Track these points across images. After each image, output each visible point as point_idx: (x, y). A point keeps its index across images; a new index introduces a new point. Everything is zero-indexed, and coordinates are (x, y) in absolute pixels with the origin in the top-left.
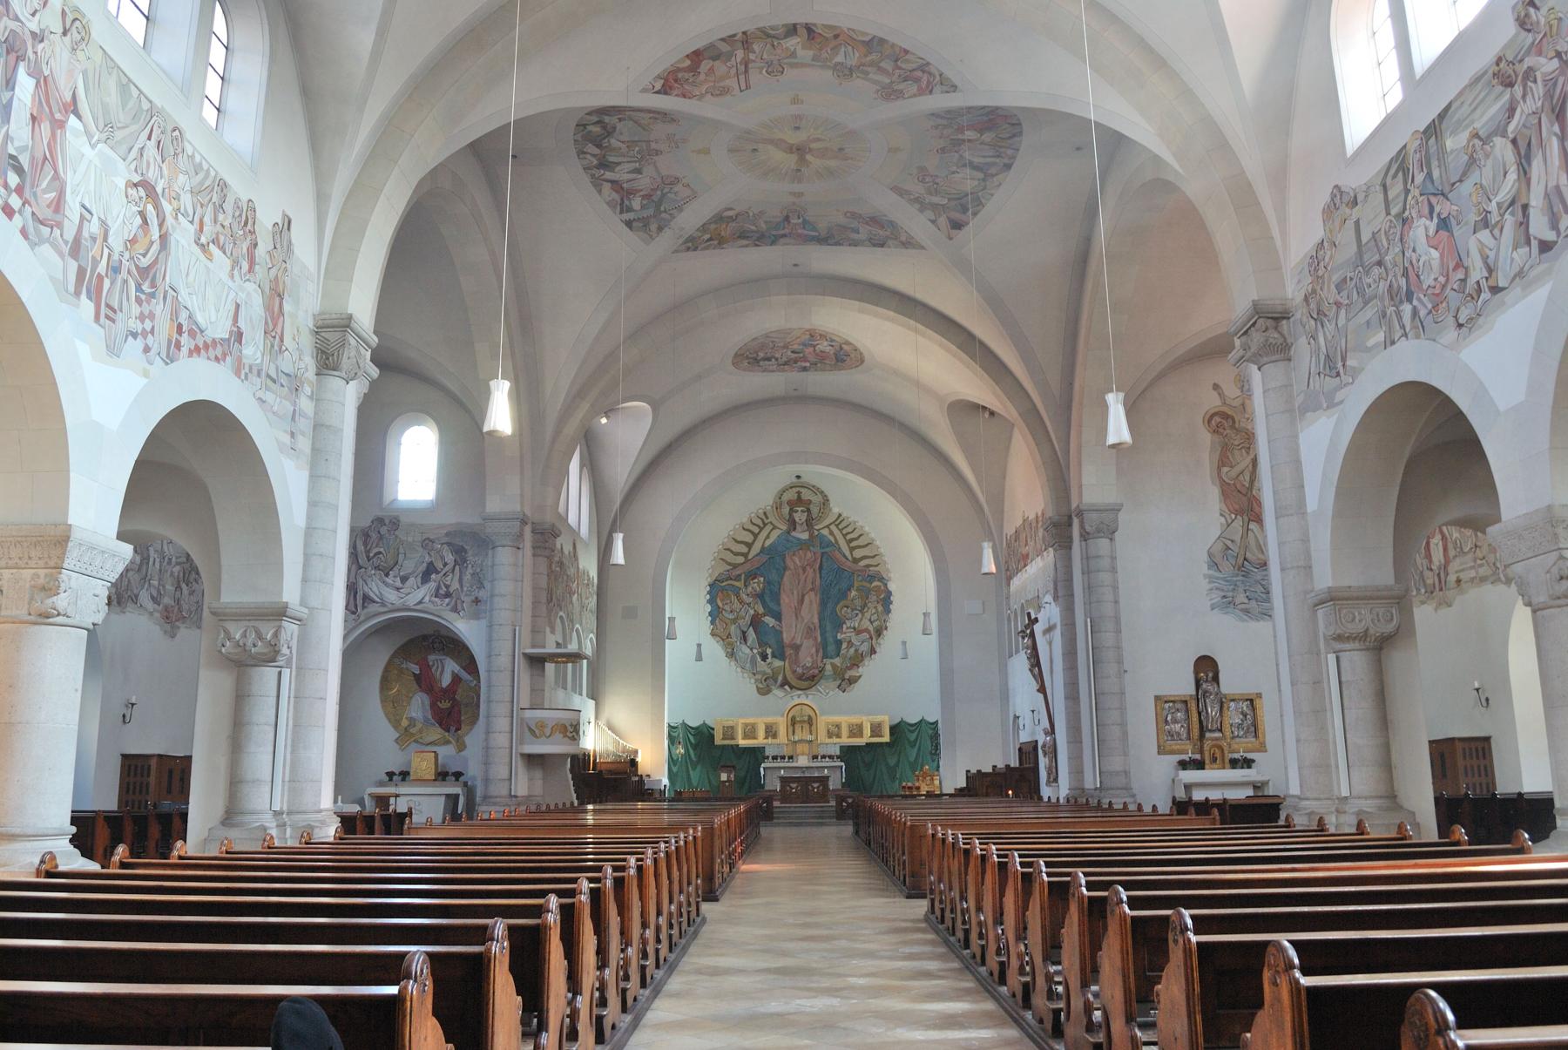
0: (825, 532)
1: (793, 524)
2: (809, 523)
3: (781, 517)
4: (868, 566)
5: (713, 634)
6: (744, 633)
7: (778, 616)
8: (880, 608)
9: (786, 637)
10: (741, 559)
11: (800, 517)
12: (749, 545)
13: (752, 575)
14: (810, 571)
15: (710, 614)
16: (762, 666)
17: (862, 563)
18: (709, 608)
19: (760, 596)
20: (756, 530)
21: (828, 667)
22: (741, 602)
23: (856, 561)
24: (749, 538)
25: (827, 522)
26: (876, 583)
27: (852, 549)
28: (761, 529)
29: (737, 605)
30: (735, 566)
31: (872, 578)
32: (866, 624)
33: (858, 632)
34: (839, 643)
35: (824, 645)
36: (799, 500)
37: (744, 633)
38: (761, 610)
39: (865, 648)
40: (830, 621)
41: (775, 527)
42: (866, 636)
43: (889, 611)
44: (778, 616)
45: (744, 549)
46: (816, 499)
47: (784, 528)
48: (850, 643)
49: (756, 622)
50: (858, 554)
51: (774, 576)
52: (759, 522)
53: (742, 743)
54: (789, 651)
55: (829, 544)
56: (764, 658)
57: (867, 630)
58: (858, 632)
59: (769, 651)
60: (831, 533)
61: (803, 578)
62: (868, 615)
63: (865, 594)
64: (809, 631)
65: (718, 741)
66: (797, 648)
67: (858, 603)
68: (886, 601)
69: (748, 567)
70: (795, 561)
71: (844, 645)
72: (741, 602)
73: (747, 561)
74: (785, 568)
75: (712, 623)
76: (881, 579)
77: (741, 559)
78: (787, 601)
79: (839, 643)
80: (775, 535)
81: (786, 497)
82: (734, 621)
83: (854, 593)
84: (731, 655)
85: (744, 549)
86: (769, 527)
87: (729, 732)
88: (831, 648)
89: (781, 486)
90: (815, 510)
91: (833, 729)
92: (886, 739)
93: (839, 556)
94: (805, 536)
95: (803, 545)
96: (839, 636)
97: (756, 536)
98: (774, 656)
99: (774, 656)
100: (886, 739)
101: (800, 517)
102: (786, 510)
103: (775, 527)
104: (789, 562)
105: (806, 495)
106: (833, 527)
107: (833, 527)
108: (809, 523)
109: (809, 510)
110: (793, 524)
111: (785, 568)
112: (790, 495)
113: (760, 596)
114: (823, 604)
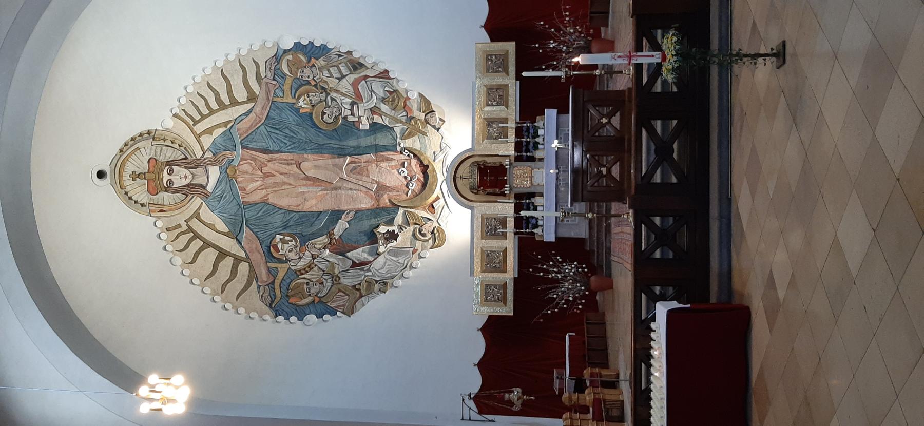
0: (207, 141)
1: (192, 189)
2: (191, 164)
3: (178, 206)
4: (259, 78)
5: (350, 312)
6: (354, 265)
7: (337, 215)
8: (321, 62)
9: (366, 203)
10: (244, 268)
11: (181, 177)
12: (223, 254)
13: (270, 253)
14: (270, 168)
15: (320, 316)
16: (404, 238)
17: (256, 88)
18: (311, 318)
19: (304, 240)
20: (198, 243)
21: (408, 143)
22: (310, 267)
23: (252, 98)
24: (210, 255)
25: (191, 140)
26: (285, 68)
27: (234, 103)
28: (197, 236)
29: (313, 275)
30: (253, 275)
31: (277, 74)
32: (345, 85)
33: (357, 99)
34: (376, 128)
35: (377, 149)
36: (153, 178)
37: (354, 265)
38: (324, 239)
39: (379, 88)
40: (342, 140)
41: (196, 215)
42: (362, 87)
43: (324, 50)
44: (337, 215)
45: (229, 261)
46: (147, 150)
47: (197, 201)
48: (374, 111)
49: (341, 248)
50: (241, 94)
51: (277, 220)
52: (184, 239)
53: (510, 274)
54: (385, 201)
55: (228, 136)
56: (392, 236)
57: (355, 85)
58: (357, 99)
59: (383, 229)
60: (209, 131)
61: (280, 178)
62: (332, 83)
63: (300, 84)
64: (356, 170)
65: (507, 310)
66: (382, 188)
67: (315, 97)
68: (311, 52)
69: (258, 258)
70: (253, 188)
71: (377, 119)
72: (310, 267)
73: (247, 259)
74: (265, 202)
75: (333, 313)
76: (277, 58)
77: (244, 268)
78: (315, 201)
79: (376, 128)
80: (208, 215)
81: (144, 197)
82: (336, 279)
83: (301, 103)
84: (384, 285)
85: (229, 261)
86: (196, 225)
87: (491, 293)
88: (382, 139)
89: (119, 204)
90: (169, 154)
91: (494, 131)
92: (510, 47)
93: (245, 124)
94: (214, 172)
95: (228, 176)
96: (365, 125)
97: (207, 244)
98: (390, 222)
99: (390, 222)
100: (510, 47)
101: (181, 177)
102: (165, 197)
103: (196, 215)
104: (256, 197)
105: (139, 162)
106: (199, 128)
107: (199, 128)
108: (191, 164)
109: (170, 163)
110: (192, 189)
111: (265, 202)
112: (139, 191)
113: (304, 240)
114: (320, 149)
